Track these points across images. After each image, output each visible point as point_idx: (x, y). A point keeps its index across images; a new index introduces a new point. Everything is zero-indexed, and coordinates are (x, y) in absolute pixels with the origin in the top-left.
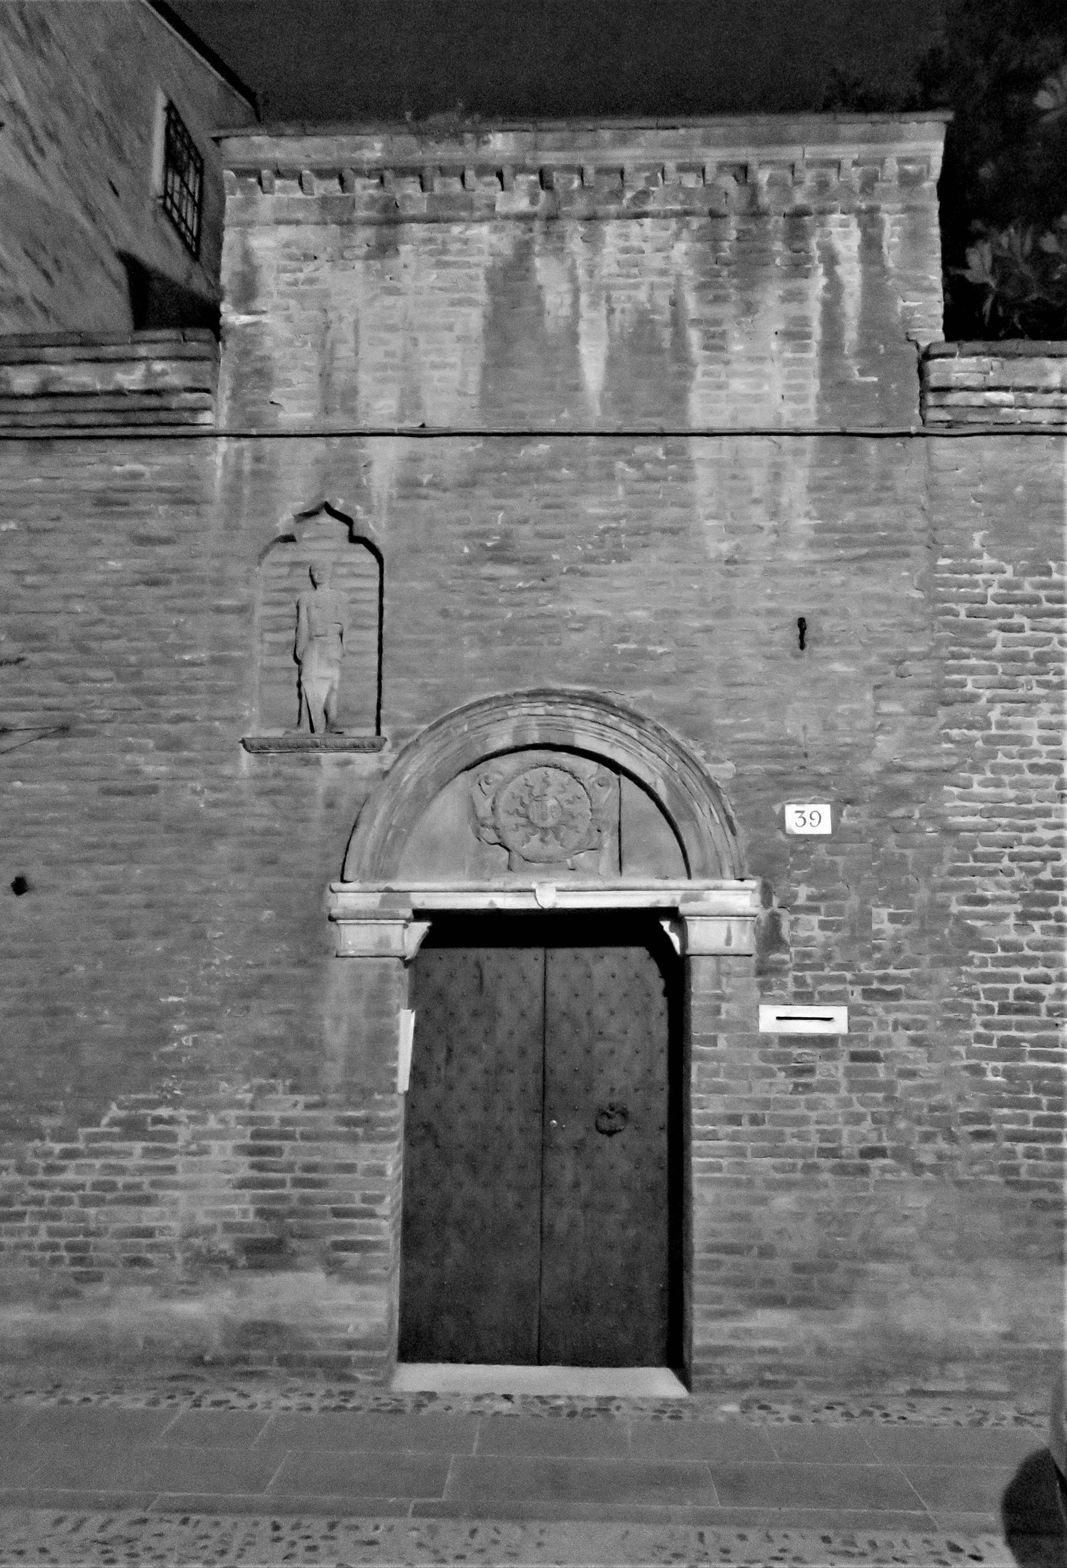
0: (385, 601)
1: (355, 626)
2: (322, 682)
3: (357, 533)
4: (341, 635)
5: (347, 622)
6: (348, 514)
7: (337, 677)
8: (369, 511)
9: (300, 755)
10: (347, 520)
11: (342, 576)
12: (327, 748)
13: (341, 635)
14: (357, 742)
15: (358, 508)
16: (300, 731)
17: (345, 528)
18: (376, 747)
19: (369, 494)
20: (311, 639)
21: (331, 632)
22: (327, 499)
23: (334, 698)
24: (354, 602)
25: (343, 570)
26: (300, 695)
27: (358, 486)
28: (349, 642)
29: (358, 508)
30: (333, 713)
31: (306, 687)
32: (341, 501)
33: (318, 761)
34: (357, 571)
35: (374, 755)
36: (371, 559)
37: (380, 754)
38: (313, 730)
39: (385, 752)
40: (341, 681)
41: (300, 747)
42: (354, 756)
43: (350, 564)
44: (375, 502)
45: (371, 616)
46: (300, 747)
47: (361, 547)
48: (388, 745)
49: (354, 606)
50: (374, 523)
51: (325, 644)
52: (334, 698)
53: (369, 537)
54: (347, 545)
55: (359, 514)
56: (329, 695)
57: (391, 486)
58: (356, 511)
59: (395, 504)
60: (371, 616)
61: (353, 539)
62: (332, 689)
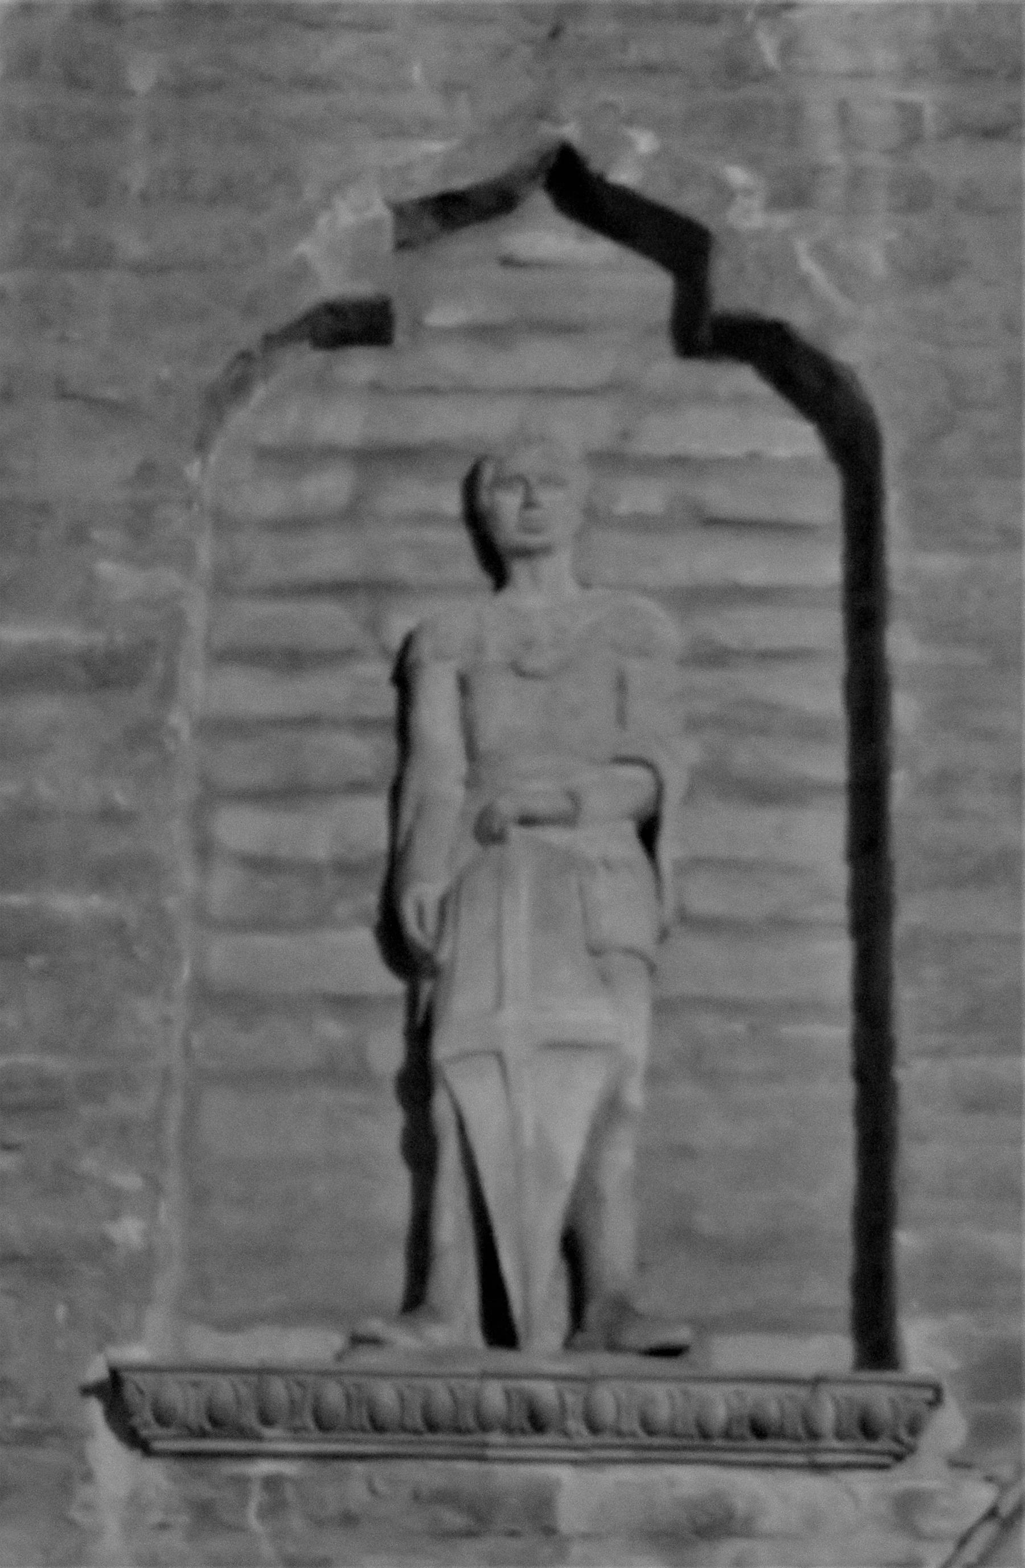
0: (902, 645)
1: (718, 781)
2: (547, 1082)
3: (732, 292)
4: (648, 832)
5: (680, 760)
6: (689, 202)
7: (638, 1046)
8: (793, 193)
9: (429, 1475)
10: (678, 244)
11: (641, 524)
12: (602, 1439)
13: (648, 832)
14: (771, 1403)
15: (737, 175)
16: (439, 1335)
17: (646, 285)
18: (879, 1439)
19: (795, 109)
20: (488, 832)
21: (596, 802)
22: (571, 132)
23: (621, 1158)
24: (712, 656)
25: (643, 496)
26: (420, 1151)
27: (737, 69)
28: (693, 865)
29: (737, 175)
30: (615, 1249)
31: (471, 1095)
32: (645, 142)
33: (539, 1514)
34: (719, 496)
35: (866, 1485)
36: (796, 439)
37: (901, 1479)
38: (499, 1326)
39: (925, 1472)
40: (655, 1076)
41: (447, 1427)
42: (746, 1486)
43: (680, 462)
44: (827, 149)
45: (808, 731)
46: (447, 1427)
47: (743, 378)
48: (949, 1427)
49: (706, 678)
50: (823, 252)
51: (569, 862)
52: (621, 1158)
53: (800, 318)
54: (667, 368)
55: (740, 207)
56: (597, 1137)
57: (912, 73)
58: (725, 193)
59: (926, 161)
60: (808, 731)
61: (704, 331)
62: (610, 1110)
